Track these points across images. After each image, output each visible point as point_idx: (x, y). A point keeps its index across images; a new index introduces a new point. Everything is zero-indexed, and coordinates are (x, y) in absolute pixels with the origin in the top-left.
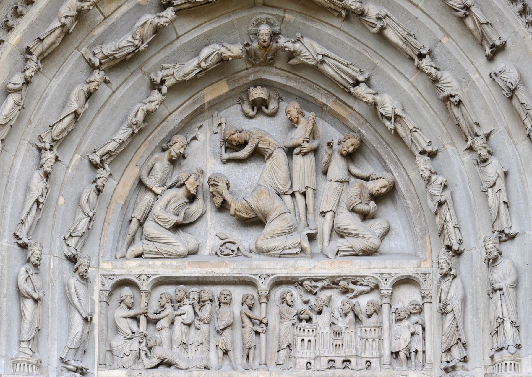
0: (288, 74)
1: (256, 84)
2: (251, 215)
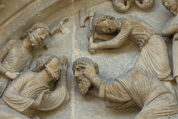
2: (126, 98)
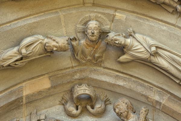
0: (117, 74)
1: (81, 82)
